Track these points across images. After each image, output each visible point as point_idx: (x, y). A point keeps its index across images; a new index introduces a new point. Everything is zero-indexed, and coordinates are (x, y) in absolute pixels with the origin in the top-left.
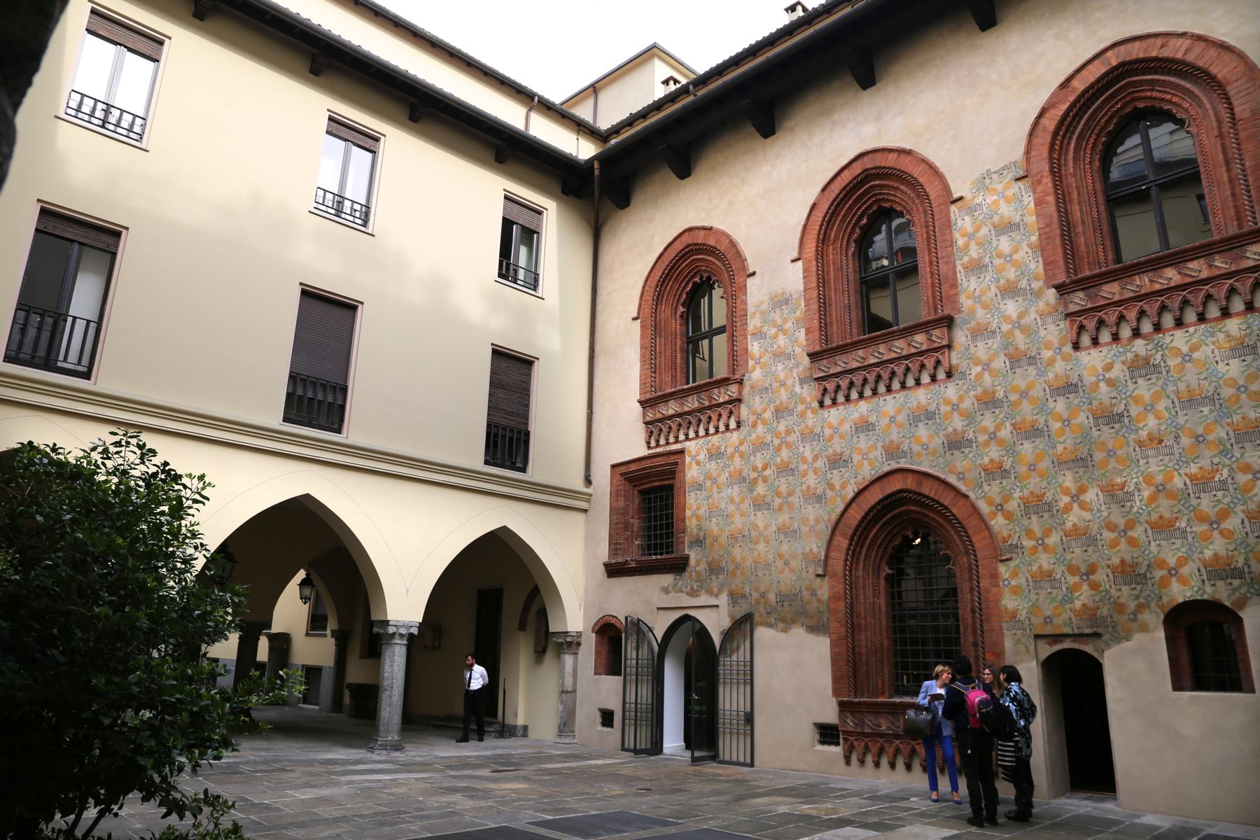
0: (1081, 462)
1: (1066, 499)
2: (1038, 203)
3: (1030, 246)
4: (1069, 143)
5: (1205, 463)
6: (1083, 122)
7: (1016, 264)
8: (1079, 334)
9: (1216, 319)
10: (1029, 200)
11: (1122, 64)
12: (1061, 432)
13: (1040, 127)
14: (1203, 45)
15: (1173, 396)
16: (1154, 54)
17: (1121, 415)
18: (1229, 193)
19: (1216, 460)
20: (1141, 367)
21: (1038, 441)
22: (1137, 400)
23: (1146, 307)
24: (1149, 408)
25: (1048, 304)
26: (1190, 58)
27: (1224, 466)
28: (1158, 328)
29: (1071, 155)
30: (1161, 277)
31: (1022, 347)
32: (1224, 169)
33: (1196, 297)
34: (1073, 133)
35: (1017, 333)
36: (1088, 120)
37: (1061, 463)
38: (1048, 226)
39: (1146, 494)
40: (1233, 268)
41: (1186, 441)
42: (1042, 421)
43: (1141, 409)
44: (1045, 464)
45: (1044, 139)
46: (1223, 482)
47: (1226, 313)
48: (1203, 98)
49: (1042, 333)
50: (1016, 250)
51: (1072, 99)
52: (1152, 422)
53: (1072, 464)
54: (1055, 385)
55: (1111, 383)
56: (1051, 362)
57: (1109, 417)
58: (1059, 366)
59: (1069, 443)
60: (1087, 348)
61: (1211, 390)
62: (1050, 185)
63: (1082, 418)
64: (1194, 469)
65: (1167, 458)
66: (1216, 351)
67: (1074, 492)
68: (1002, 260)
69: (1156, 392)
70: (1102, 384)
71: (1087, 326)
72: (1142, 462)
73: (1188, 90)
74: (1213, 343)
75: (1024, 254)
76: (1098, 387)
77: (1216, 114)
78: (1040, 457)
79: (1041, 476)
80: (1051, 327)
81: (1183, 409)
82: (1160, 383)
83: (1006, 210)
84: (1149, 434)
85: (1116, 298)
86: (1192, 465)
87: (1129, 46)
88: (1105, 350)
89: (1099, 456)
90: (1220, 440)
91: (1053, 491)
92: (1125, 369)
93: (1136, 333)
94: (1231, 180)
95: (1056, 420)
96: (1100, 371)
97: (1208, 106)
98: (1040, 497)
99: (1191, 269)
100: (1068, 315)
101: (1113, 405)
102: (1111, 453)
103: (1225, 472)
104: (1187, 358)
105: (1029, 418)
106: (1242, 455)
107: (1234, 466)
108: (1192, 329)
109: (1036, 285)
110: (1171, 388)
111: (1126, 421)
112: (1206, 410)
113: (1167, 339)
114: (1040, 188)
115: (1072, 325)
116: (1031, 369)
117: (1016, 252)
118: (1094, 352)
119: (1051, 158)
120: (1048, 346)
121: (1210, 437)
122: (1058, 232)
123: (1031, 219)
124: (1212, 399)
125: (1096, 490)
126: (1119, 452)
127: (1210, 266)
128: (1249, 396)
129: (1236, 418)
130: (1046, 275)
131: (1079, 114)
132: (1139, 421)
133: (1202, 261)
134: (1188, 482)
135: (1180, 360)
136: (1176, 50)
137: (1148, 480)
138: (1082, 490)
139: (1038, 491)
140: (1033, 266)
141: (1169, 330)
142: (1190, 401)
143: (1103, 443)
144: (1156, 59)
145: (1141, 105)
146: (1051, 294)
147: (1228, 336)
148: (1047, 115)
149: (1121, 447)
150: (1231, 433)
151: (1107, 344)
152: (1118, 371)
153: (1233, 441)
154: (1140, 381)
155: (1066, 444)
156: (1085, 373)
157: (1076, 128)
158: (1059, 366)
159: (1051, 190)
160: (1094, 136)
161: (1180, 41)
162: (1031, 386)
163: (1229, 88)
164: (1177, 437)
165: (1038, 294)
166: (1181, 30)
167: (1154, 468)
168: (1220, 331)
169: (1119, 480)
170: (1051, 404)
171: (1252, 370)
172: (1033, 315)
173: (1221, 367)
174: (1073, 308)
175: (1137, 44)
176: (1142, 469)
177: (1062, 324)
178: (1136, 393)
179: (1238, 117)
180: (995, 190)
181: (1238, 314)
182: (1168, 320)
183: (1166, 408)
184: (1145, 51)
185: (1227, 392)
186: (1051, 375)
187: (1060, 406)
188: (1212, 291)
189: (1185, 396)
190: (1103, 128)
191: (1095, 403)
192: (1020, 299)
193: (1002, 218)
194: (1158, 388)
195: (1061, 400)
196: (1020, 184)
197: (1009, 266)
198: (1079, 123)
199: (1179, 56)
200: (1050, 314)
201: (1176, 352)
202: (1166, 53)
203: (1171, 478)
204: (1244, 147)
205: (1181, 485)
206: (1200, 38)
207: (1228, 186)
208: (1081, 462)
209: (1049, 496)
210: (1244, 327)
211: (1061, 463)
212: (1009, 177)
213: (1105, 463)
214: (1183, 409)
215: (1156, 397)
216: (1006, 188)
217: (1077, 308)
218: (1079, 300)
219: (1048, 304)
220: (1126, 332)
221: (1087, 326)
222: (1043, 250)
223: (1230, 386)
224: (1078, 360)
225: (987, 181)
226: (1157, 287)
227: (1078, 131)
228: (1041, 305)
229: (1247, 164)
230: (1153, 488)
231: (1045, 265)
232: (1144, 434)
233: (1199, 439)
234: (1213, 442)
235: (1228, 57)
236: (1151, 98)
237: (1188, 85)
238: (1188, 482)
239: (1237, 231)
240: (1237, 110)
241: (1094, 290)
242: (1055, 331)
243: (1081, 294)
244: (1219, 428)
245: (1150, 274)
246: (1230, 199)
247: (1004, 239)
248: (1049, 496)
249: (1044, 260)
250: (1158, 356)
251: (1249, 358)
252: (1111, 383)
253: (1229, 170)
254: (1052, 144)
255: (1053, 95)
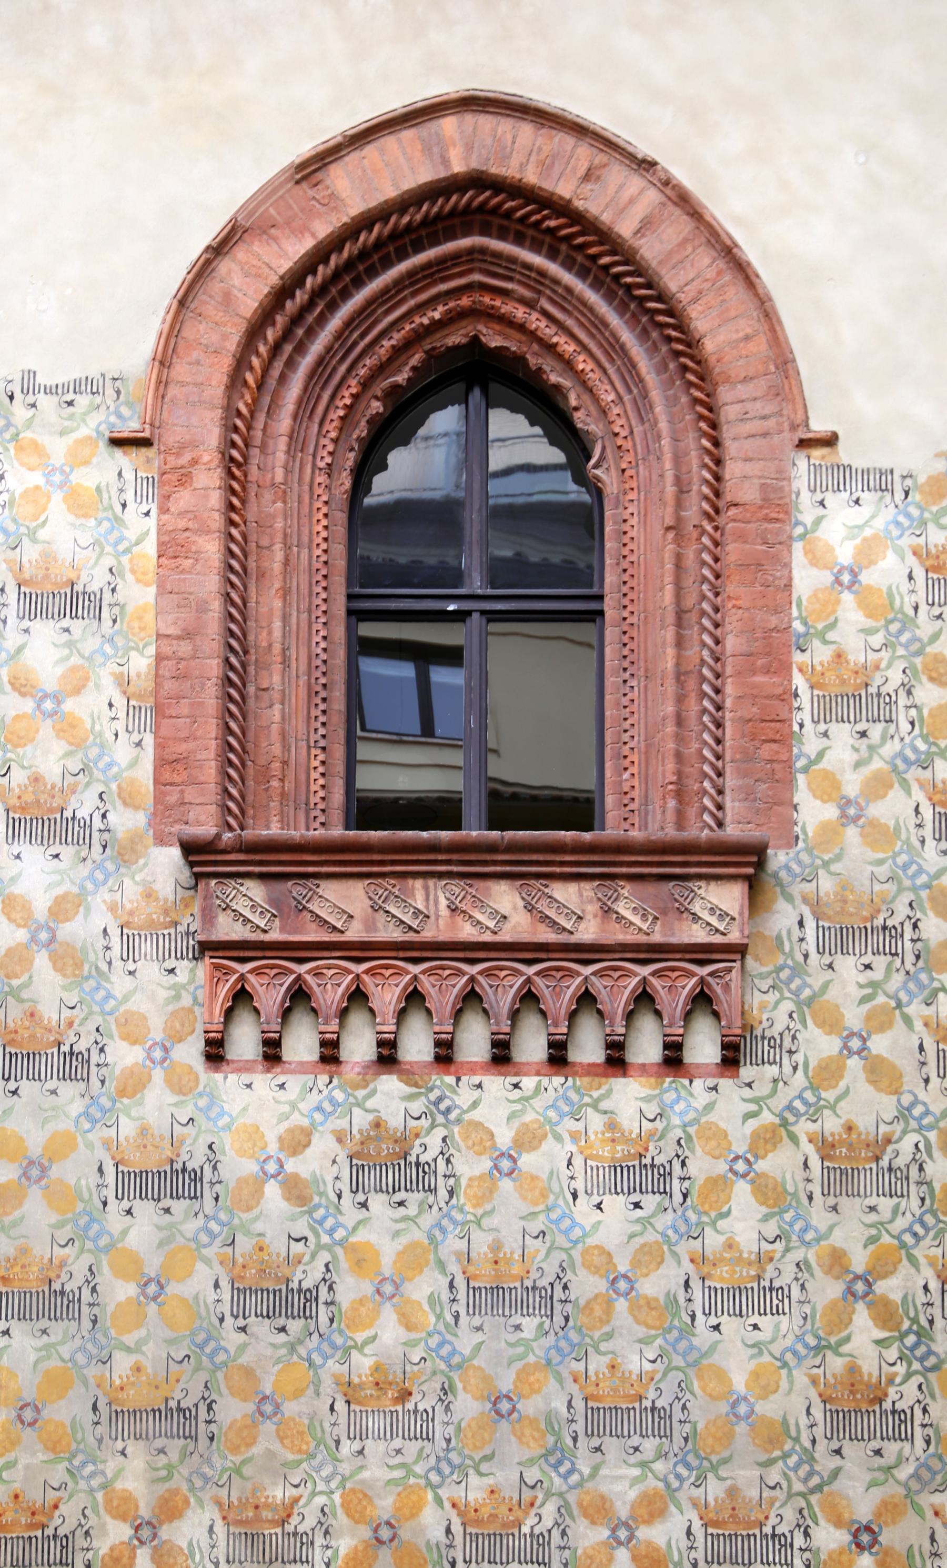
0: (181, 1419)
1: (118, 1532)
2: (171, 548)
3: (124, 683)
4: (283, 379)
5: (505, 1477)
6: (335, 322)
7: (68, 728)
8: (229, 1014)
9: (591, 1070)
10: (142, 527)
11: (477, 181)
12: (134, 1314)
13: (214, 287)
14: (686, 225)
15: (454, 1268)
16: (564, 189)
17: (310, 1296)
18: (670, 709)
19: (532, 1476)
20: (388, 1165)
21: (58, 1329)
22: (362, 1259)
23: (427, 985)
24: (389, 1290)
25: (149, 895)
26: (650, 250)
27: (548, 1495)
28: (445, 1055)
29: (284, 423)
30: (479, 902)
31: (50, 1013)
32: (670, 634)
33: (557, 992)
34: (300, 349)
35: (42, 961)
36: (349, 324)
37: (120, 1416)
38: (187, 635)
39: (344, 1545)
40: (657, 937)
41: (467, 1406)
42: (79, 1269)
43: (368, 1288)
44: (70, 1410)
45: (220, 333)
46: (541, 1540)
47: (616, 1060)
48: (656, 394)
49: (120, 983)
50: (77, 683)
51: (323, 229)
52: (389, 1332)
53: (149, 1425)
54: (137, 1161)
55: (298, 1192)
56: (132, 1086)
57: (282, 1298)
58: (157, 1104)
59: (152, 1355)
60: (245, 1067)
61: (551, 1270)
62: (216, 499)
63: (201, 1283)
64: (475, 1491)
65: (412, 1447)
66: (578, 1162)
67: (145, 1512)
68: (28, 705)
69: (413, 1246)
70: (272, 1190)
71: (261, 991)
72: (348, 1448)
73: (623, 350)
74: (575, 1137)
75: (98, 705)
76: (258, 1193)
77: (678, 460)
78: (56, 1383)
79: (53, 1446)
80: (150, 971)
81: (473, 1309)
82: (428, 1220)
83: (64, 541)
84: (377, 1368)
85: (355, 933)
86: (474, 1479)
87: (505, 126)
88: (295, 1083)
89: (232, 1410)
90: (550, 1417)
91: (81, 1500)
92: (342, 1158)
93: (387, 1057)
94: (680, 676)
95: (120, 1273)
96: (273, 1148)
97: (663, 425)
98: (39, 1516)
99: (561, 906)
100: (206, 948)
101: (292, 1261)
102: (266, 1406)
103: (549, 1511)
104: (505, 1164)
105: (41, 1250)
106: (596, 1469)
107: (572, 1498)
108: (529, 1083)
109: (127, 821)
110: (453, 1244)
111: (324, 1315)
112: (530, 1324)
113: (464, 1096)
114: (183, 499)
115: (215, 983)
116: (68, 1090)
117: (77, 690)
118: (263, 1081)
119: (231, 412)
120: (132, 1029)
121: (530, 1406)
122: (214, 667)
123: (140, 595)
124: (547, 1298)
125: (211, 1513)
126: (290, 1408)
127: (607, 911)
128: (634, 1309)
129: (597, 1364)
130: (159, 799)
131: (329, 295)
132: (356, 1323)
133: (588, 888)
134: (457, 1528)
135: (486, 1164)
136: (621, 205)
137: (357, 1502)
138: (170, 1509)
139: (35, 1496)
140: (122, 752)
141: (473, 1069)
142: (495, 1293)
143: (249, 1373)
144: (563, 209)
145: (494, 341)
146: (167, 863)
147: (612, 1126)
148: (240, 253)
149: (297, 1394)
150: (579, 1404)
151: (302, 1068)
152: (321, 1161)
153: (579, 1427)
154: (378, 1202)
155: (141, 1355)
156: (227, 1144)
157: (311, 333)
158: (157, 1104)
159: (216, 520)
160: (353, 386)
161: (635, 182)
162: (60, 1147)
163: (724, 394)
164: (446, 1391)
165: (125, 854)
166: (644, 149)
167: (376, 1471)
168: (595, 1106)
169: (278, 1493)
170: (114, 1217)
171: (651, 1237)
172: (100, 918)
173: (583, 1209)
174: (228, 929)
175: (526, 131)
176: (345, 1468)
177: (184, 967)
178: (360, 1236)
179: (731, 491)
180: (37, 448)
181: (644, 1069)
182: (474, 1041)
183: (431, 1298)
184: (545, 166)
185: (586, 1285)
186: (128, 1128)
187: (141, 1229)
188: (599, 986)
189: (485, 1276)
190: (381, 370)
191: (244, 1244)
192: (67, 852)
193: (48, 558)
194: (418, 1235)
195: (145, 1210)
196: (123, 459)
197: (46, 729)
198: (322, 320)
199: (625, 229)
200: (151, 924)
201: (483, 1138)
202: (593, 203)
203: (416, 1510)
204: (731, 588)
205: (438, 1534)
206: (683, 200)
207: (670, 687)
208: (181, 1419)
209: (67, 1518)
210: (651, 1110)
211: (120, 1416)
212: (96, 421)
213: (246, 1434)
214: (473, 1309)
215: (414, 1260)
216: (78, 459)
217: (238, 932)
218: (247, 908)
219: (149, 895)
220: (359, 1046)
221: (261, 991)
222: (159, 710)
223: (595, 1270)
224: (213, 1098)
225: (20, 412)
226: (467, 932)
227: (316, 348)
228: (131, 891)
229: (731, 643)
230: (366, 1532)
231: (162, 763)
232: (363, 1363)
233: (501, 1406)
234: (533, 1422)
235: (736, 293)
236: (521, 328)
237: (627, 336)
238: (457, 1528)
239: (670, 833)
240: (732, 470)
241: (295, 889)
242: (163, 991)
243: (256, 890)
244: (552, 1383)
245: (456, 887)
246: (670, 729)
247: (45, 632)
248: (67, 1518)
249: (160, 746)
250: (434, 1141)
251: (650, 1201)
252: (298, 1192)
253: (680, 643)
254: (241, 364)
255: (268, 192)
